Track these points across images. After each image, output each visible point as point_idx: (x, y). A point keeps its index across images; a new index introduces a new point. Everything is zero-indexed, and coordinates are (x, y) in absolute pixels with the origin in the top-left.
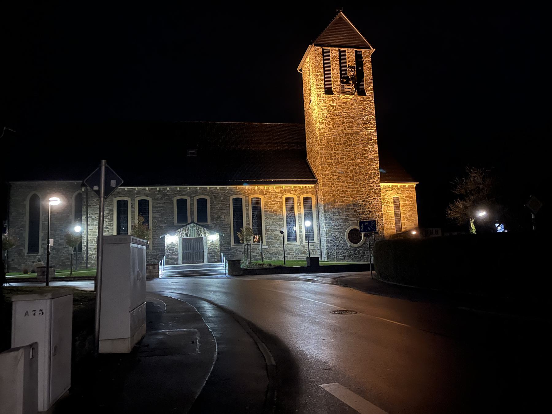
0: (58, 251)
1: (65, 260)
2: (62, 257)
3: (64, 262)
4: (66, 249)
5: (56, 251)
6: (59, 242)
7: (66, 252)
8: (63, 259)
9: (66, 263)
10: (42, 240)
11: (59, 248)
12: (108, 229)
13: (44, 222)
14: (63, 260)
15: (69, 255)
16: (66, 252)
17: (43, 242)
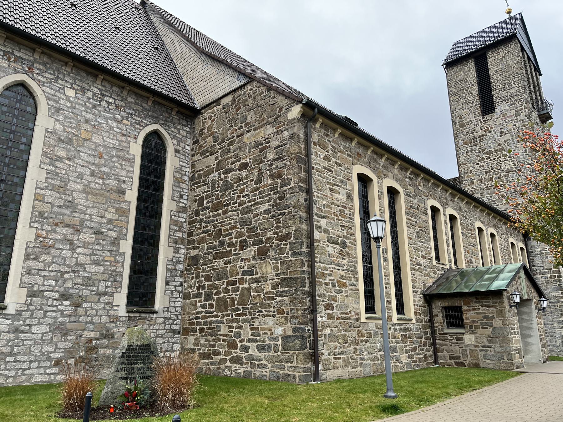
0: (78, 305)
1: (98, 339)
2: (91, 327)
3: (95, 348)
4: (104, 299)
5: (70, 305)
6: (85, 271)
7: (104, 308)
8: (92, 334)
9: (101, 351)
10: (27, 257)
11: (86, 292)
12: (347, 249)
13: (43, 192)
14: (91, 341)
15: (112, 322)
16: (104, 308)
17: (30, 263)
